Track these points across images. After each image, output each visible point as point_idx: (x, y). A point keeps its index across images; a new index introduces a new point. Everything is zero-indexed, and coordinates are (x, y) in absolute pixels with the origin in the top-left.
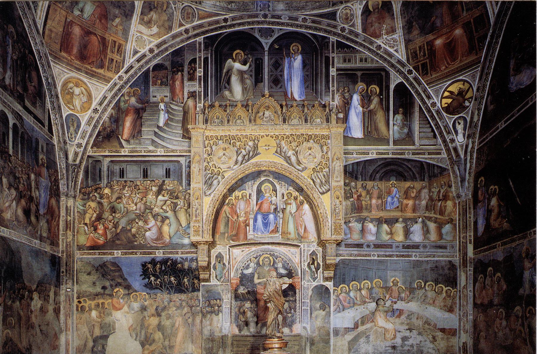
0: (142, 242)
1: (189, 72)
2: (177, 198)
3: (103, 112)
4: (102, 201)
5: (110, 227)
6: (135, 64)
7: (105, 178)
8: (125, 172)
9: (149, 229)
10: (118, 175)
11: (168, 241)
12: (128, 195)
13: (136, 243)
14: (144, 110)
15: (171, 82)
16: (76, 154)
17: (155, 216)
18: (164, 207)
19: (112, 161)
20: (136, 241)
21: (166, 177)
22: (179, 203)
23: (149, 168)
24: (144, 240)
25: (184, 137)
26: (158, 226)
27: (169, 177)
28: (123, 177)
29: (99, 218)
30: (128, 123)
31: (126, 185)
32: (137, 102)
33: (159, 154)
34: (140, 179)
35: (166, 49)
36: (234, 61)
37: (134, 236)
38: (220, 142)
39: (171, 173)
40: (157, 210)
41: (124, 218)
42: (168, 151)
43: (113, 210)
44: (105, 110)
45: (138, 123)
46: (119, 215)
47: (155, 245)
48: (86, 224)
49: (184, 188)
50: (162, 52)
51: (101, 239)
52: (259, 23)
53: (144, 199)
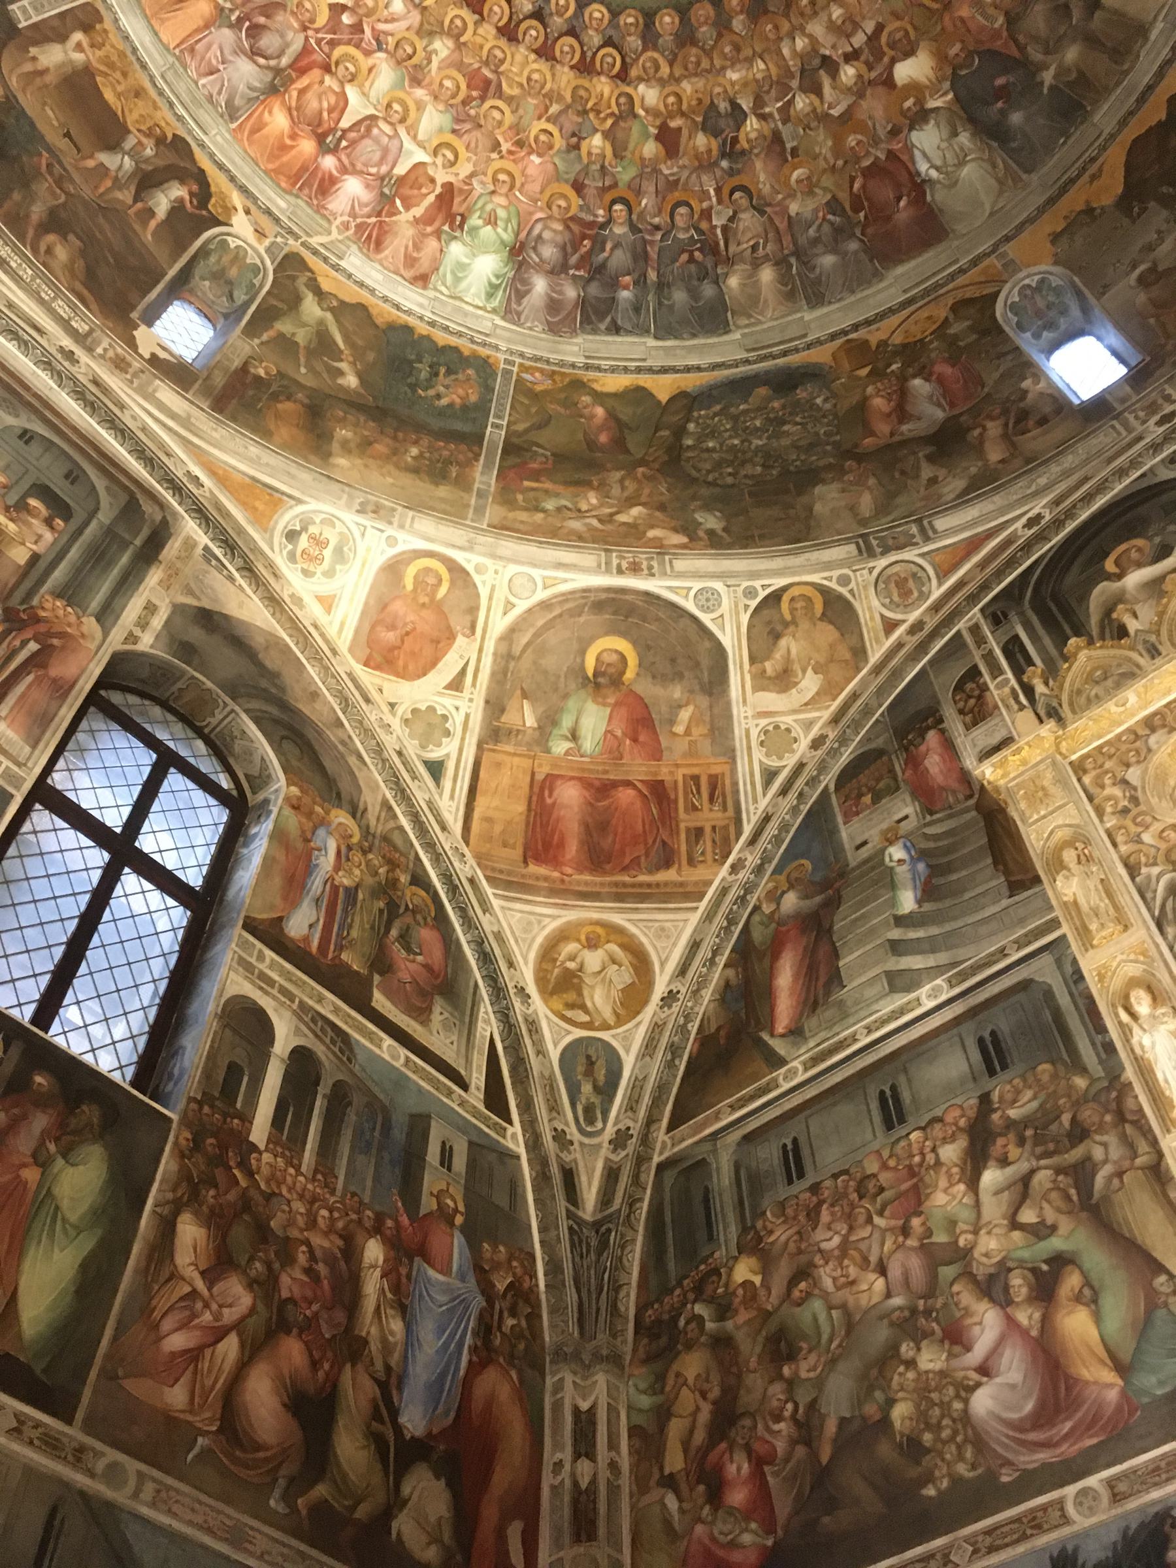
0: (962, 1469)
1: (961, 712)
2: (1079, 1133)
3: (696, 993)
4: (729, 1325)
5: (780, 1446)
6: (776, 805)
7: (731, 1217)
8: (805, 1152)
9: (985, 1370)
10: (781, 1178)
11: (1112, 1395)
12: (836, 1240)
13: (930, 1491)
14: (833, 903)
15: (909, 772)
16: (611, 1175)
17: (993, 1287)
18: (1028, 1216)
19: (747, 1138)
20: (929, 1479)
21: (992, 1072)
22: (1098, 1153)
23: (902, 1080)
24: (969, 1453)
25: (1015, 887)
26: (1024, 1333)
27: (1004, 1067)
28: (801, 1175)
29: (726, 1417)
30: (785, 978)
31: (820, 1203)
32: (806, 897)
33: (930, 1004)
34: (876, 1146)
35: (867, 712)
36: (1120, 577)
37: (913, 1448)
38: (1152, 740)
39: (1008, 1042)
40: (990, 1246)
41: (842, 1366)
42: (963, 976)
43: (782, 1346)
44: (702, 983)
45: (823, 950)
46: (812, 1358)
47: (1042, 1456)
48: (669, 1482)
49: (1097, 1070)
50: (856, 725)
51: (747, 1538)
52: (1156, 447)
53: (916, 1222)
